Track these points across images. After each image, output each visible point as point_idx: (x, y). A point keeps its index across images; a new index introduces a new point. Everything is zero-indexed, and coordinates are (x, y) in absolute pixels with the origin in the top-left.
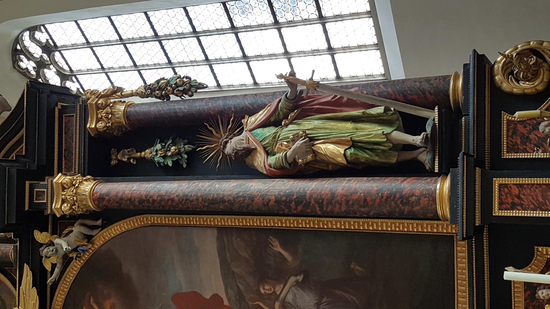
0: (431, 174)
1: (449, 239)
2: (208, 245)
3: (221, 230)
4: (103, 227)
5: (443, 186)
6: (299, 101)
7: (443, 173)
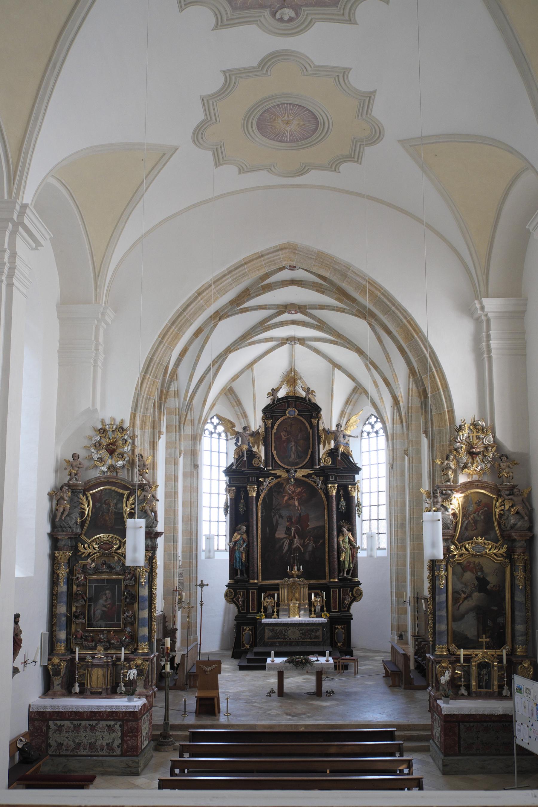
0: (338, 576)
1: (325, 579)
2: (321, 524)
3: (324, 527)
4: (324, 492)
5: (336, 580)
6: (354, 549)
7: (338, 579)
